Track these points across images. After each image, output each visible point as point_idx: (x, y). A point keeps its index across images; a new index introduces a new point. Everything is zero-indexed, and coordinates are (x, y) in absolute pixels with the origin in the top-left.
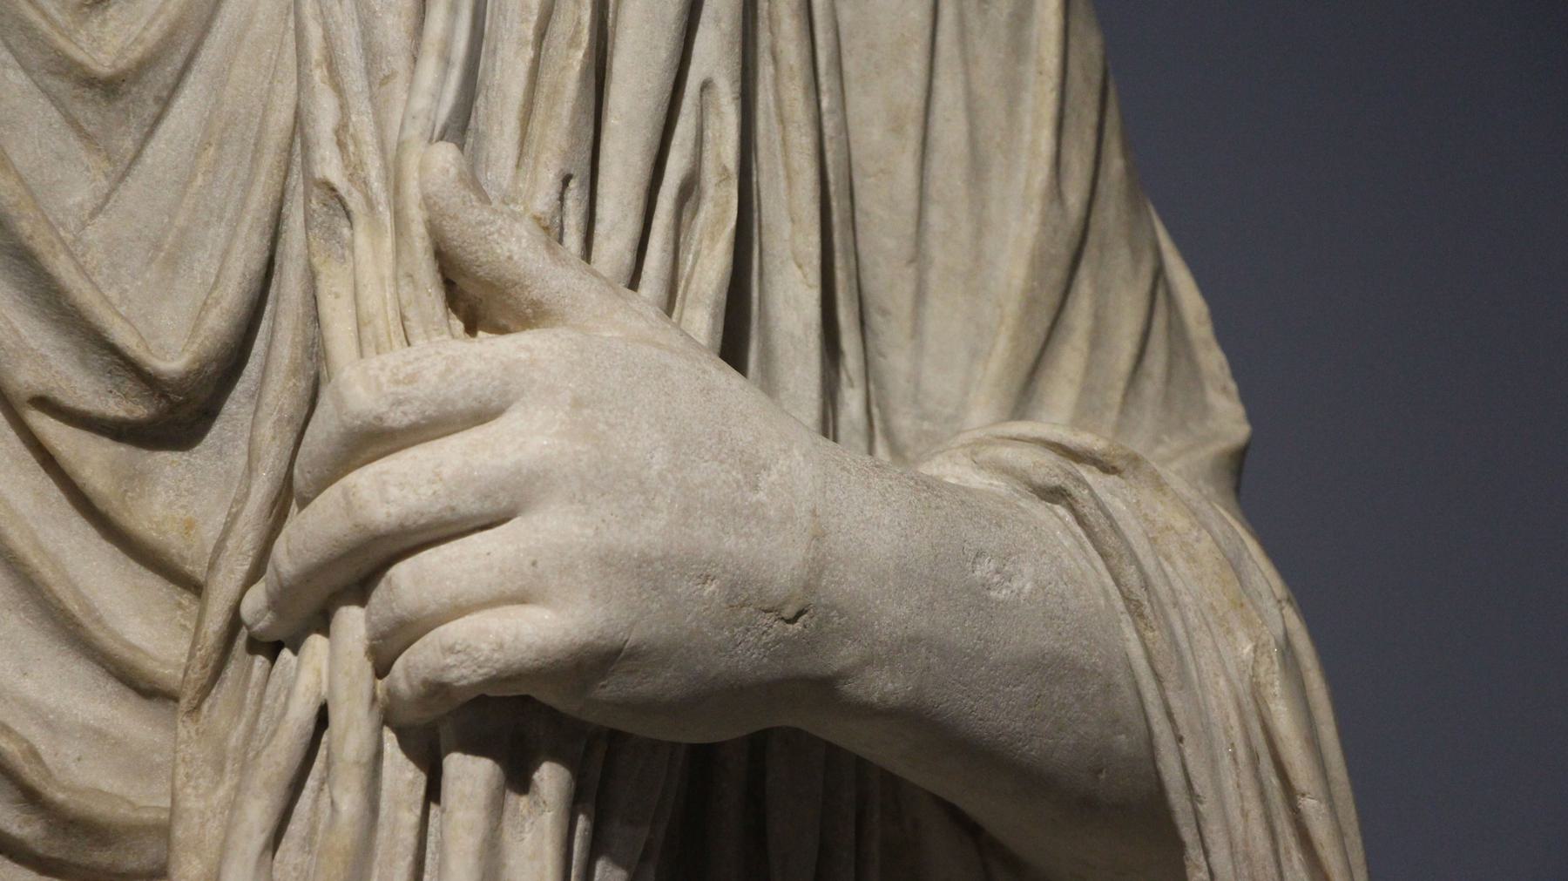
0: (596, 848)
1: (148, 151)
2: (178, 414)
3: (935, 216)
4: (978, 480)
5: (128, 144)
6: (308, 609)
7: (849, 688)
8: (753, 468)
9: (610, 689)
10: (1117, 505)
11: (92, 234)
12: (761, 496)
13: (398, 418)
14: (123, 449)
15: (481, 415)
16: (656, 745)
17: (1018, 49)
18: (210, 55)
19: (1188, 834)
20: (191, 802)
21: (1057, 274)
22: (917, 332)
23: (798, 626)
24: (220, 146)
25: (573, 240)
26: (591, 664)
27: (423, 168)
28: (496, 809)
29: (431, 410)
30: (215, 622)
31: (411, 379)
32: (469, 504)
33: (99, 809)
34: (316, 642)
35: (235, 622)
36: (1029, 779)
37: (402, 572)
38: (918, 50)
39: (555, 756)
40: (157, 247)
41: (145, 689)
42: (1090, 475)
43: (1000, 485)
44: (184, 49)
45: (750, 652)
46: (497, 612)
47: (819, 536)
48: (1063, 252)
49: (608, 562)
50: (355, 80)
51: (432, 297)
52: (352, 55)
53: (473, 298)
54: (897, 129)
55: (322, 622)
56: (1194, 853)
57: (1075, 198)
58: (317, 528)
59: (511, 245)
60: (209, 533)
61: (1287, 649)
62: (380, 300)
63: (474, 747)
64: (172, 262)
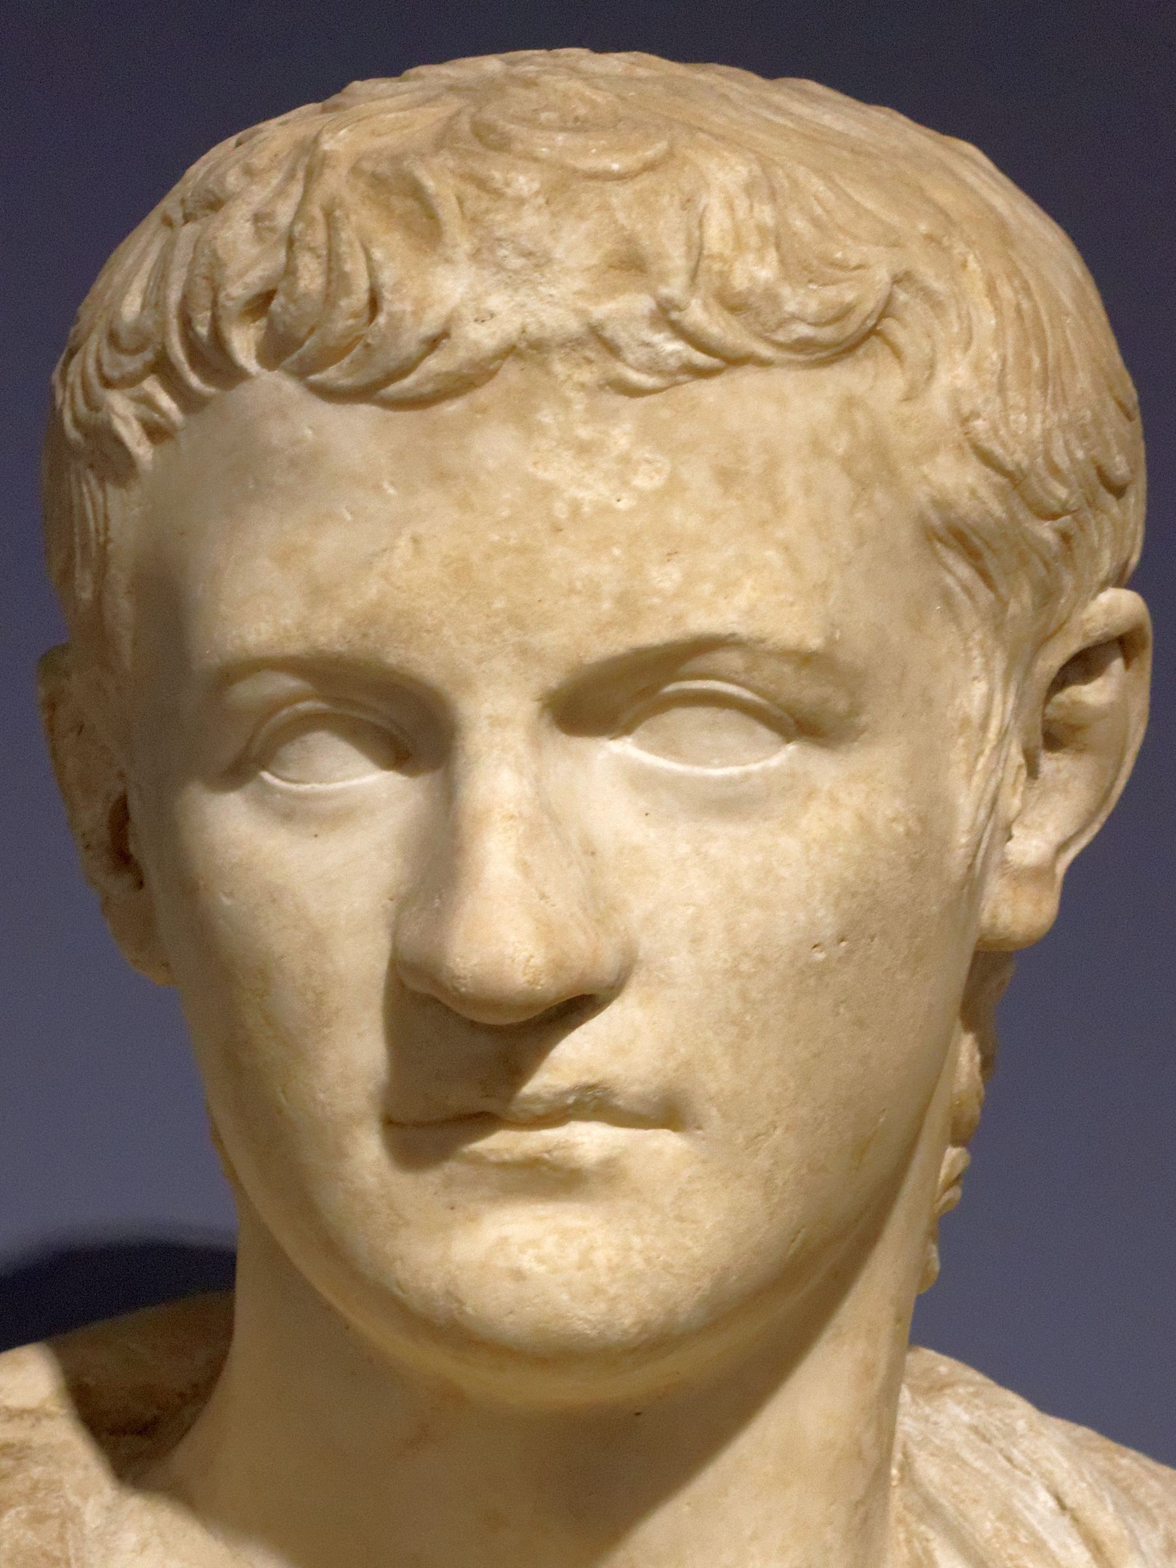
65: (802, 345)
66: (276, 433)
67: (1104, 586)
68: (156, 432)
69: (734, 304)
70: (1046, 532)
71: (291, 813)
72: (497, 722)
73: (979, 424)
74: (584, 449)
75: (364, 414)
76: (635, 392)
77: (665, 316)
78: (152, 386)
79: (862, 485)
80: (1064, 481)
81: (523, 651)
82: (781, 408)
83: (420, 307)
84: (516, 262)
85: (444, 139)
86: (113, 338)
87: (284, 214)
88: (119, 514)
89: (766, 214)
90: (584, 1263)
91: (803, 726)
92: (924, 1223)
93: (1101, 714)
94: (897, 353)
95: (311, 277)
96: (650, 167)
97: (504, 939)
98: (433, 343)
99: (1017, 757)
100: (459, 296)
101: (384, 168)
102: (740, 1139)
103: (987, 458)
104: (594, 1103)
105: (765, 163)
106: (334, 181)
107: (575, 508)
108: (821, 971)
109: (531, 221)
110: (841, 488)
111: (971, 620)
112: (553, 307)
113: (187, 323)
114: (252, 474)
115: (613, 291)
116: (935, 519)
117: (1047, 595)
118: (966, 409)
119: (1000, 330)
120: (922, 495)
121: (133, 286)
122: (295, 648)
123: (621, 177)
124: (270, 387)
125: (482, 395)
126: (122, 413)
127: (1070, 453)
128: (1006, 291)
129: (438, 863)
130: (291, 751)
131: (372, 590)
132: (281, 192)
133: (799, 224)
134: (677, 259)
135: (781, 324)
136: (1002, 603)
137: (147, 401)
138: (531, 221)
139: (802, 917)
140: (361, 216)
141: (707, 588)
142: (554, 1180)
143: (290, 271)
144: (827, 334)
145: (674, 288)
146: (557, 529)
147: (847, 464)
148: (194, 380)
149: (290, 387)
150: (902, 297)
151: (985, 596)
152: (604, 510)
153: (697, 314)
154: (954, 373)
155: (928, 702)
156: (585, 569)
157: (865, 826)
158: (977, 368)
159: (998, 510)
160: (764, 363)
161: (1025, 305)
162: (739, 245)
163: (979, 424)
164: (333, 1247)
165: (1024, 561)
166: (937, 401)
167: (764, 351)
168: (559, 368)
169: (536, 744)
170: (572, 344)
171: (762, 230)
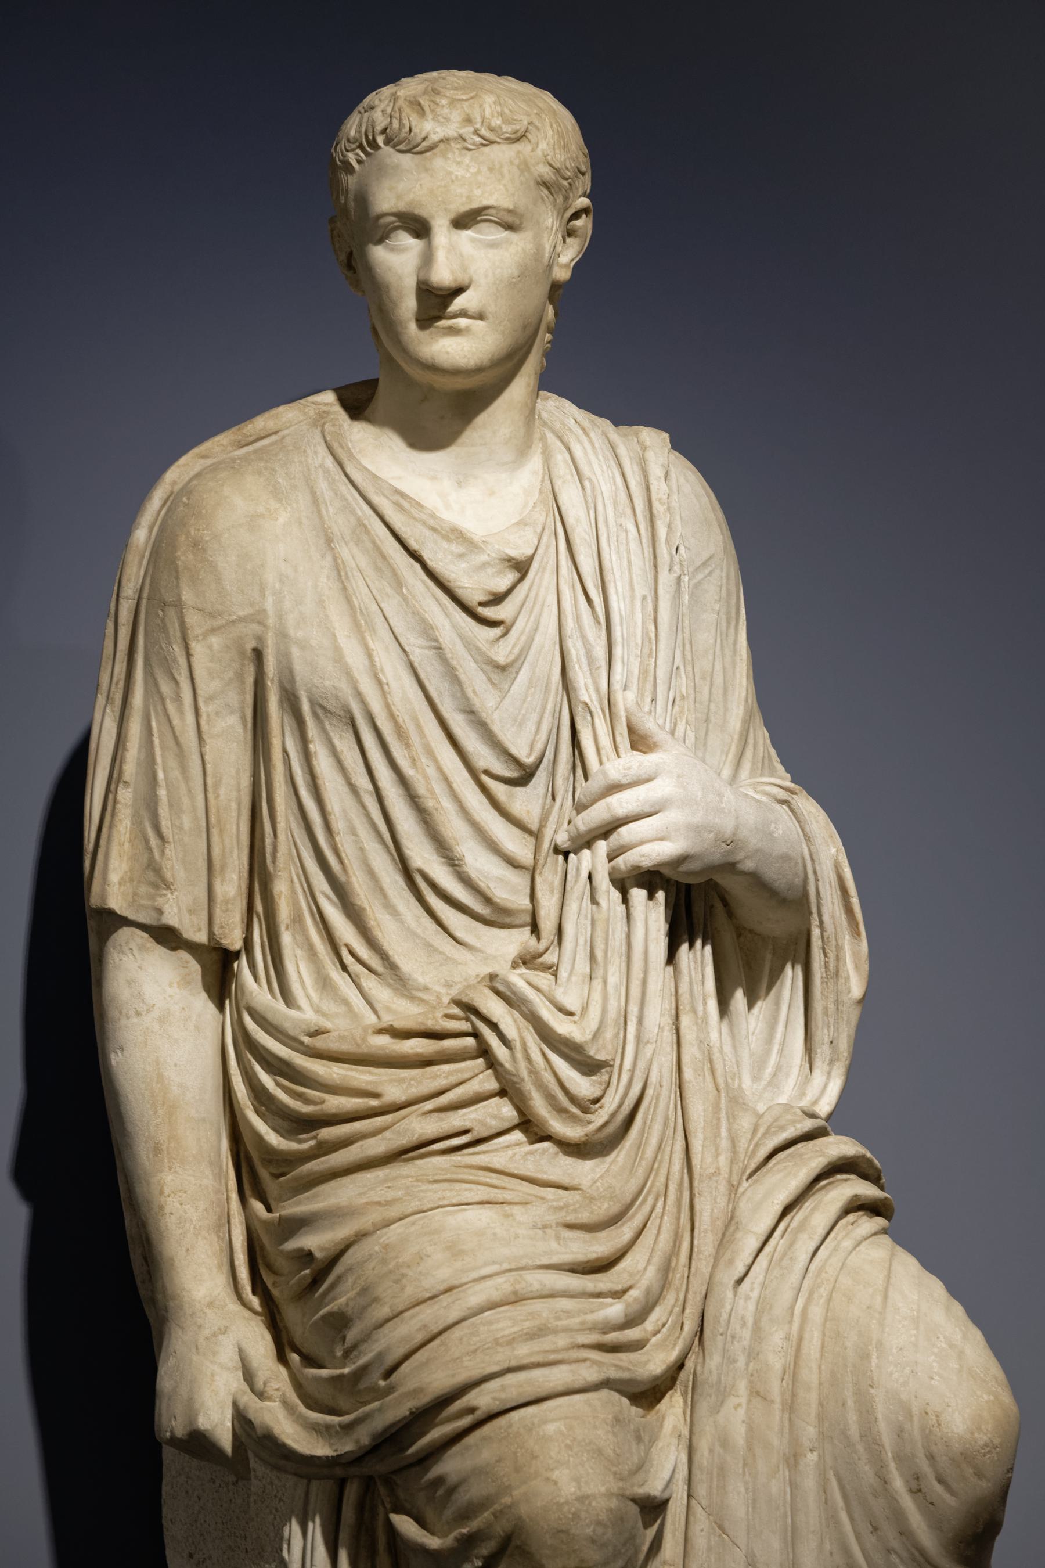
2: (524, 776)
3: (713, 706)
5: (506, 687)
6: (586, 841)
7: (741, 867)
8: (721, 795)
9: (683, 868)
13: (625, 781)
15: (648, 780)
19: (814, 910)
22: (705, 745)
26: (682, 859)
27: (624, 699)
29: (635, 779)
31: (629, 768)
32: (647, 809)
33: (509, 905)
34: (586, 853)
37: (623, 830)
39: (662, 889)
40: (515, 720)
46: (654, 844)
53: (639, 741)
54: (704, 678)
55: (589, 844)
56: (815, 916)
59: (649, 724)
62: (605, 740)
63: (640, 886)
64: (520, 725)
65: (507, 139)
66: (388, 161)
68: (359, 162)
69: (492, 130)
70: (565, 183)
71: (393, 249)
72: (440, 226)
74: (458, 163)
75: (409, 155)
77: (476, 132)
78: (358, 151)
79: (522, 171)
81: (446, 210)
82: (502, 153)
83: (421, 130)
85: (425, 92)
86: (349, 140)
87: (389, 110)
88: (351, 182)
89: (499, 109)
90: (462, 350)
91: (509, 227)
92: (541, 352)
93: (580, 228)
95: (396, 124)
96: (472, 98)
97: (443, 275)
98: (424, 139)
99: (560, 238)
100: (429, 128)
101: (412, 99)
103: (551, 165)
104: (463, 314)
105: (498, 97)
106: (400, 102)
107: (457, 177)
109: (446, 110)
111: (548, 204)
112: (451, 130)
113: (366, 135)
114: (382, 170)
115: (464, 127)
116: (539, 179)
117: (566, 198)
119: (553, 136)
120: (536, 174)
121: (353, 127)
122: (394, 210)
124: (386, 150)
126: (352, 158)
128: (554, 126)
129: (427, 259)
130: (392, 235)
131: (411, 196)
132: (388, 105)
133: (506, 111)
134: (479, 119)
136: (555, 200)
137: (357, 154)
138: (446, 110)
140: (407, 110)
143: (391, 123)
144: (513, 136)
145: (478, 126)
147: (518, 167)
148: (369, 149)
149: (391, 150)
151: (551, 198)
152: (463, 177)
153: (484, 132)
154: (543, 146)
155: (538, 223)
156: (459, 191)
160: (499, 143)
162: (493, 116)
164: (404, 350)
166: (539, 152)
167: (499, 140)
168: (453, 144)
169: (449, 231)
170: (455, 139)
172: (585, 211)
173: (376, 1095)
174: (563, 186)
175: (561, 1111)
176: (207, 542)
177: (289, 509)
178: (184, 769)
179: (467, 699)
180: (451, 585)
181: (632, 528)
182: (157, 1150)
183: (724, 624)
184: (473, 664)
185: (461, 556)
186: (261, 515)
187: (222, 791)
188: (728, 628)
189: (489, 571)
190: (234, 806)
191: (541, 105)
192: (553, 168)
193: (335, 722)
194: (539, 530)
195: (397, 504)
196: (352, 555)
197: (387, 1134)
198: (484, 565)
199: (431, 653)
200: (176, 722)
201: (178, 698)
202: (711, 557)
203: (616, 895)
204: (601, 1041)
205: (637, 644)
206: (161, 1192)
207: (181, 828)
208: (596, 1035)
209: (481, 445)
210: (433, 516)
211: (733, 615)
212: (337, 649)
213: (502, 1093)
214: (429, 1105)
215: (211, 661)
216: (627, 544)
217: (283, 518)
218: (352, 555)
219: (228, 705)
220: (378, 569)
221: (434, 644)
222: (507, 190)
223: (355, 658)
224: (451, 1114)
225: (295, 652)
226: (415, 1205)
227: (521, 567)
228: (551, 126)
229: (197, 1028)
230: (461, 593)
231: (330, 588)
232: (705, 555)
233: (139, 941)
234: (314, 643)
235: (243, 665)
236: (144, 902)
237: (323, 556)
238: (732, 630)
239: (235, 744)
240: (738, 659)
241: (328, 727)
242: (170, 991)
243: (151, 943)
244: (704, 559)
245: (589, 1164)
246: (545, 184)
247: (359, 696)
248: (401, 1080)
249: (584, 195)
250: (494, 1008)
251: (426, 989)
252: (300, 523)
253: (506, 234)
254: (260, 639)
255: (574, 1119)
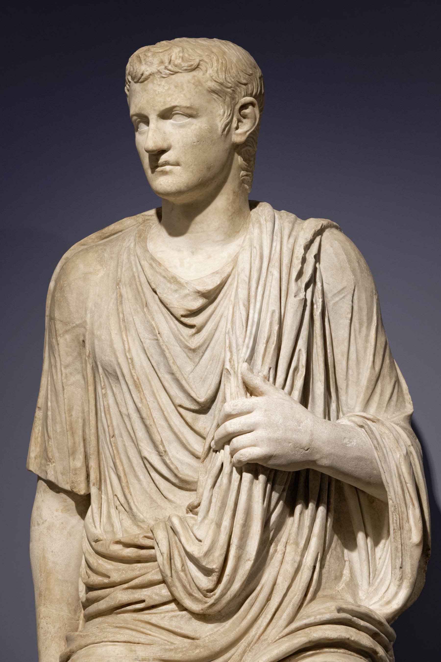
0: (272, 489)
1: (201, 361)
2: (204, 408)
3: (350, 371)
4: (349, 423)
5: (197, 360)
7: (319, 463)
8: (299, 422)
9: (271, 462)
10: (374, 429)
11: (191, 376)
12: (301, 428)
13: (234, 413)
14: (194, 414)
15: (249, 412)
16: (285, 472)
17: (367, 340)
18: (211, 345)
19: (387, 489)
20: (201, 479)
21: (373, 382)
22: (347, 392)
23: (308, 451)
24: (213, 361)
25: (271, 379)
27: (241, 367)
28: (252, 483)
29: (239, 411)
30: (207, 446)
31: (236, 406)
32: (245, 429)
33: (187, 478)
35: (210, 448)
36: (358, 479)
37: (234, 440)
38: (347, 341)
39: (263, 473)
40: (202, 378)
41: (198, 458)
42: (369, 422)
43: (352, 424)
44: (207, 344)
45: (298, 456)
46: (252, 448)
47: (312, 435)
48: (374, 379)
49: (270, 440)
50: (234, 350)
51: (242, 390)
52: (234, 345)
54: (343, 356)
57: (377, 368)
58: (222, 431)
59: (257, 381)
60: (208, 429)
61: (408, 455)
62: (234, 390)
63: (248, 471)
64: (204, 381)
65: (186, 70)
67: (244, 97)
68: (128, 90)
69: (176, 66)
71: (140, 133)
72: (152, 119)
73: (214, 77)
74: (159, 85)
75: (138, 84)
76: (164, 78)
77: (166, 68)
80: (230, 83)
81: (154, 110)
83: (140, 70)
84: (149, 64)
89: (181, 55)
90: (168, 182)
91: (190, 116)
93: (249, 114)
94: (202, 70)
99: (235, 119)
100: (144, 69)
102: (187, 166)
103: (215, 81)
104: (167, 163)
107: (158, 92)
108: (196, 146)
109: (150, 59)
110: (193, 87)
112: (154, 69)
116: (209, 90)
117: (233, 98)
118: (211, 75)
120: (206, 87)
123: (161, 52)
125: (148, 80)
127: (231, 80)
133: (186, 55)
134: (167, 61)
135: (182, 67)
139: (191, 139)
141: (173, 100)
142: (165, 173)
145: (167, 64)
146: (157, 95)
147: (194, 84)
150: (201, 62)
151: (221, 99)
152: (162, 92)
153: (170, 67)
154: (210, 71)
155: (212, 112)
156: (160, 99)
157: (200, 128)
158: (213, 70)
159: (218, 88)
160: (181, 72)
161: (224, 62)
162: (176, 59)
163: (214, 77)
165: (226, 94)
167: (180, 71)
168: (156, 76)
169: (157, 121)
170: (157, 73)
171: (180, 57)
172: (252, 104)
173: (109, 577)
174: (229, 92)
175: (190, 595)
176: (65, 287)
177: (105, 269)
178: (57, 402)
179: (170, 367)
180: (168, 306)
181: (276, 274)
182: (40, 595)
183: (357, 325)
184: (179, 349)
185: (176, 291)
186: (91, 273)
187: (74, 413)
188: (360, 328)
189: (190, 298)
190: (80, 421)
191: (215, 50)
192: (217, 82)
193: (112, 378)
194: (225, 275)
195: (151, 265)
196: (127, 293)
197: (107, 599)
198: (186, 295)
199: (155, 342)
200: (55, 377)
201: (56, 366)
202: (343, 289)
203: (236, 475)
204: (211, 558)
205: (264, 337)
206: (39, 617)
207: (56, 432)
208: (207, 554)
209: (202, 232)
210: (166, 270)
211: (365, 319)
212: (111, 341)
213: (164, 581)
214: (126, 586)
215: (67, 347)
216: (271, 282)
217: (101, 274)
218: (127, 293)
219: (76, 369)
220: (136, 299)
221: (155, 337)
222: (185, 96)
223: (118, 346)
224: (139, 591)
225: (96, 342)
226: (93, 639)
227: (211, 297)
228: (218, 60)
229: (70, 534)
230: (172, 310)
231: (113, 309)
232: (340, 287)
233: (43, 487)
234: (103, 337)
235: (80, 349)
236: (43, 468)
237: (113, 293)
238: (364, 329)
239: (80, 389)
240: (369, 345)
241: (110, 381)
242: (56, 514)
243: (48, 489)
244: (339, 290)
245: (210, 626)
246: (214, 91)
247: (119, 364)
248: (119, 570)
249: (251, 95)
250: (161, 535)
251: (143, 521)
252: (109, 276)
253: (190, 119)
254: (84, 336)
255: (196, 600)
